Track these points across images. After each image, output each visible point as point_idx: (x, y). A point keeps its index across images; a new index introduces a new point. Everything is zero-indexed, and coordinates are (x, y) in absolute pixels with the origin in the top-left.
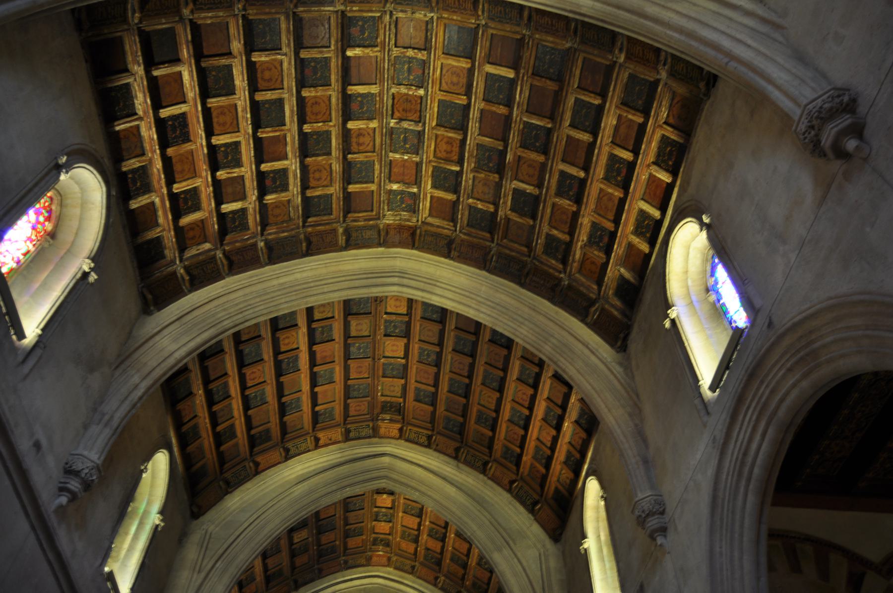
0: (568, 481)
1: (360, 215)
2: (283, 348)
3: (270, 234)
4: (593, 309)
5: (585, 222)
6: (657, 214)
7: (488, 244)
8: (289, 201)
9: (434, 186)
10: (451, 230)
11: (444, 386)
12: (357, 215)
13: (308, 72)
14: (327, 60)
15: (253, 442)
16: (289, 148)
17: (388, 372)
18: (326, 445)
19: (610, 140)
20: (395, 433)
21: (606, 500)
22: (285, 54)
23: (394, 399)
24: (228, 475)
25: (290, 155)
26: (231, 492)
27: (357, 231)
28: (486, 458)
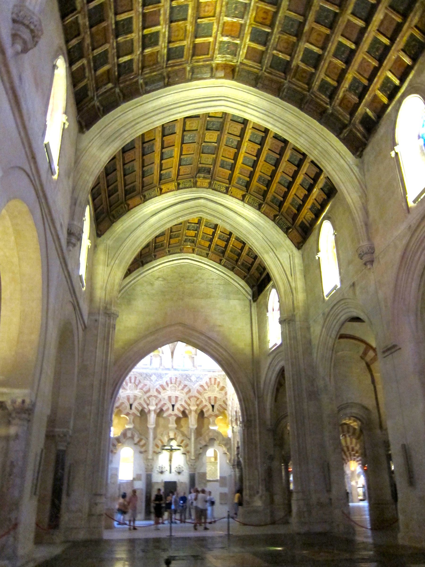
0: (310, 219)
3: (146, 74)
4: (345, 131)
5: (349, 76)
6: (397, 82)
7: (282, 80)
8: (158, 52)
9: (251, 40)
10: (258, 69)
11: (240, 160)
15: (127, 192)
16: (161, 18)
17: (205, 151)
18: (166, 192)
19: (377, 28)
20: (206, 184)
21: (335, 235)
23: (207, 166)
24: (113, 212)
25: (162, 22)
26: (116, 221)
27: (198, 68)
28: (261, 201)
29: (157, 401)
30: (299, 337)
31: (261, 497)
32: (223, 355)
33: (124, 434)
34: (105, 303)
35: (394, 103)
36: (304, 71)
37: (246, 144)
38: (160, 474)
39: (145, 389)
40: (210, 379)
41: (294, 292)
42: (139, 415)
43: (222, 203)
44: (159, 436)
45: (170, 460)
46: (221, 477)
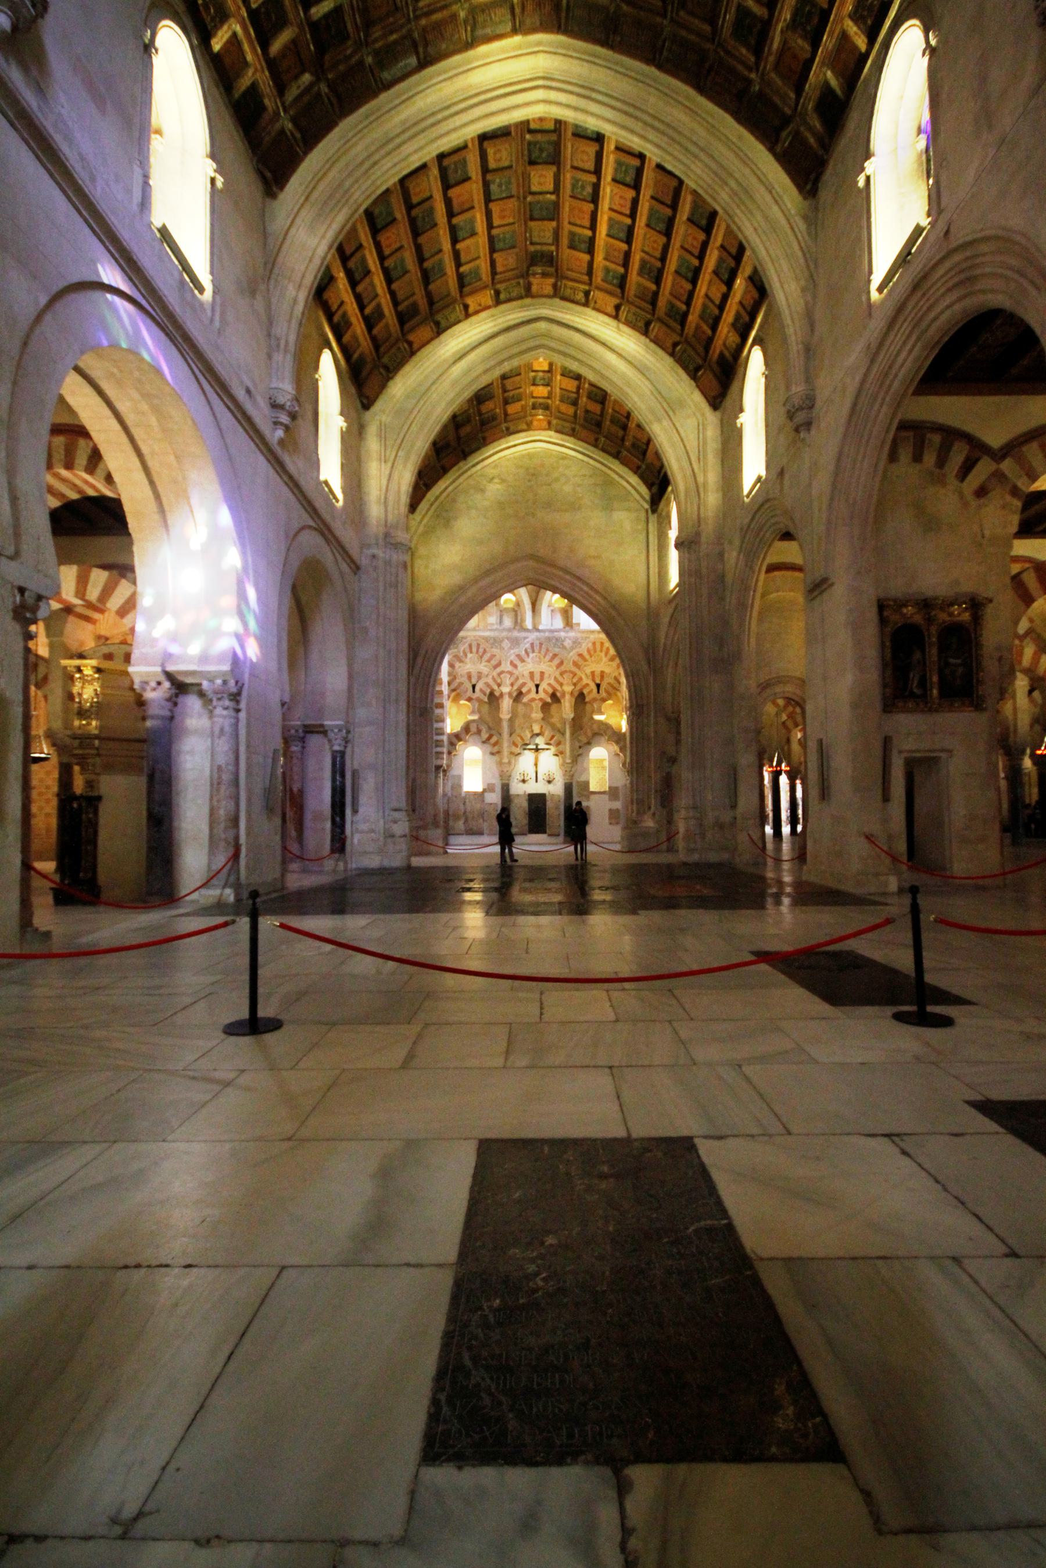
2: (415, 200)
4: (784, 134)
7: (659, 19)
15: (403, 319)
17: (536, 214)
18: (477, 312)
20: (549, 290)
23: (545, 248)
24: (385, 360)
29: (512, 679)
30: (704, 571)
31: (654, 814)
32: (599, 603)
33: (466, 728)
34: (386, 526)
35: (877, 46)
37: (608, 190)
38: (521, 784)
39: (494, 662)
40: (594, 644)
41: (701, 490)
42: (486, 700)
43: (580, 326)
44: (518, 731)
45: (536, 765)
46: (610, 788)
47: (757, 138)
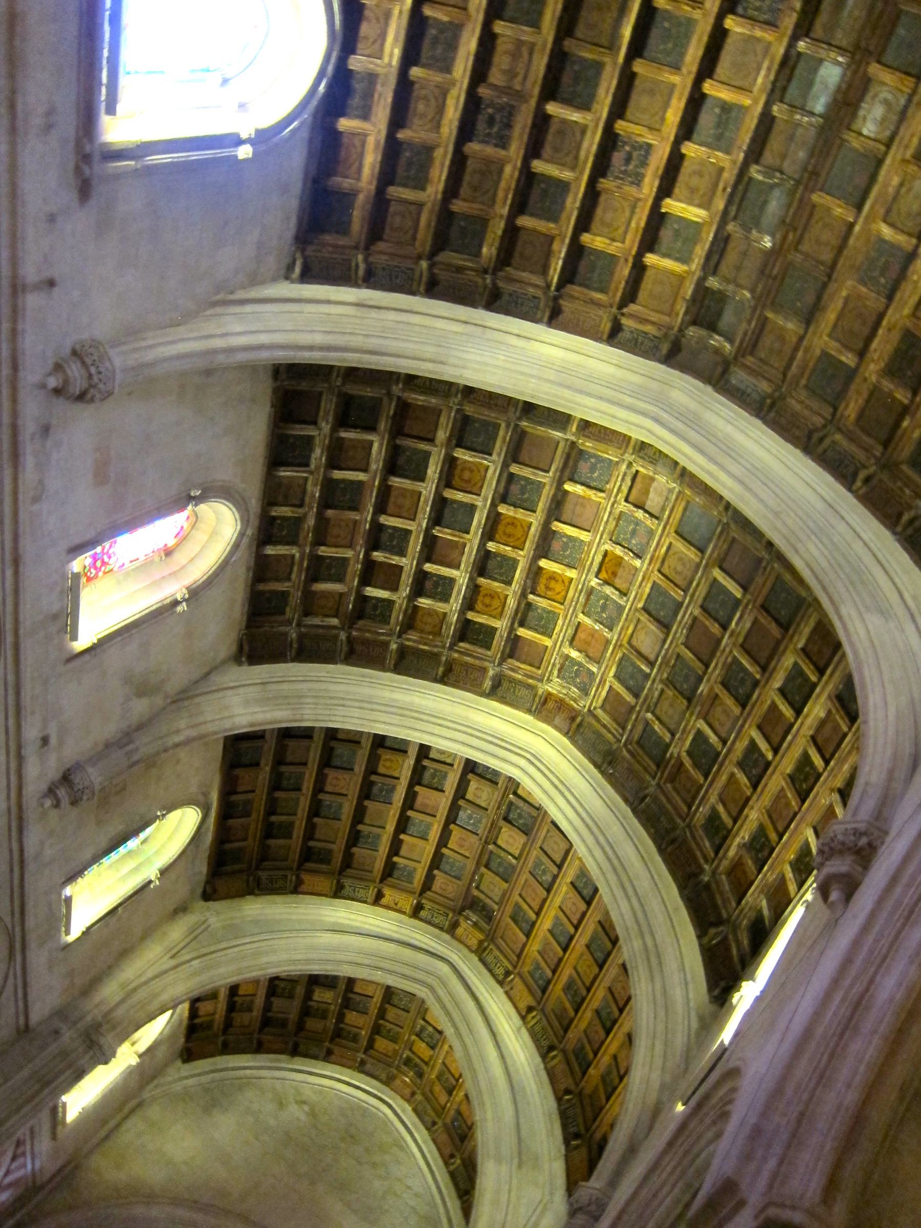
1: (522, 666)
3: (408, 640)
4: (712, 931)
7: (648, 778)
8: (445, 614)
12: (518, 664)
13: (515, 489)
14: (541, 485)
16: (464, 559)
18: (387, 907)
19: (811, 732)
20: (474, 943)
22: (493, 462)
23: (488, 901)
24: (263, 875)
26: (257, 895)
36: (690, 778)
47: (692, 920)
